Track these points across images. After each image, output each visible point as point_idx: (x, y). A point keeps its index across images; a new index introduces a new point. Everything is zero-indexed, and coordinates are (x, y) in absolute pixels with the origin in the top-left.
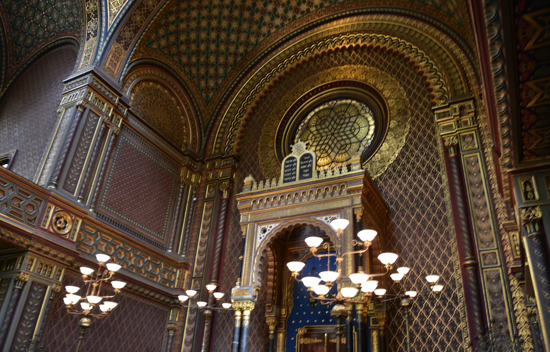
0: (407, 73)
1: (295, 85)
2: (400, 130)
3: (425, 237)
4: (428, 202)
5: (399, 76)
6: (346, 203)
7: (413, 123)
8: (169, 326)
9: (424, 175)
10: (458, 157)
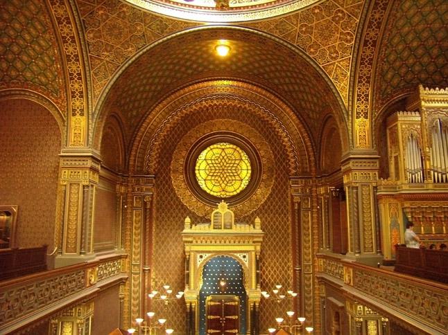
0: (275, 141)
1: (197, 124)
2: (268, 183)
3: (277, 251)
4: (280, 231)
5: (270, 141)
6: (252, 248)
7: (276, 179)
8: (120, 296)
9: (280, 214)
10: (299, 210)
